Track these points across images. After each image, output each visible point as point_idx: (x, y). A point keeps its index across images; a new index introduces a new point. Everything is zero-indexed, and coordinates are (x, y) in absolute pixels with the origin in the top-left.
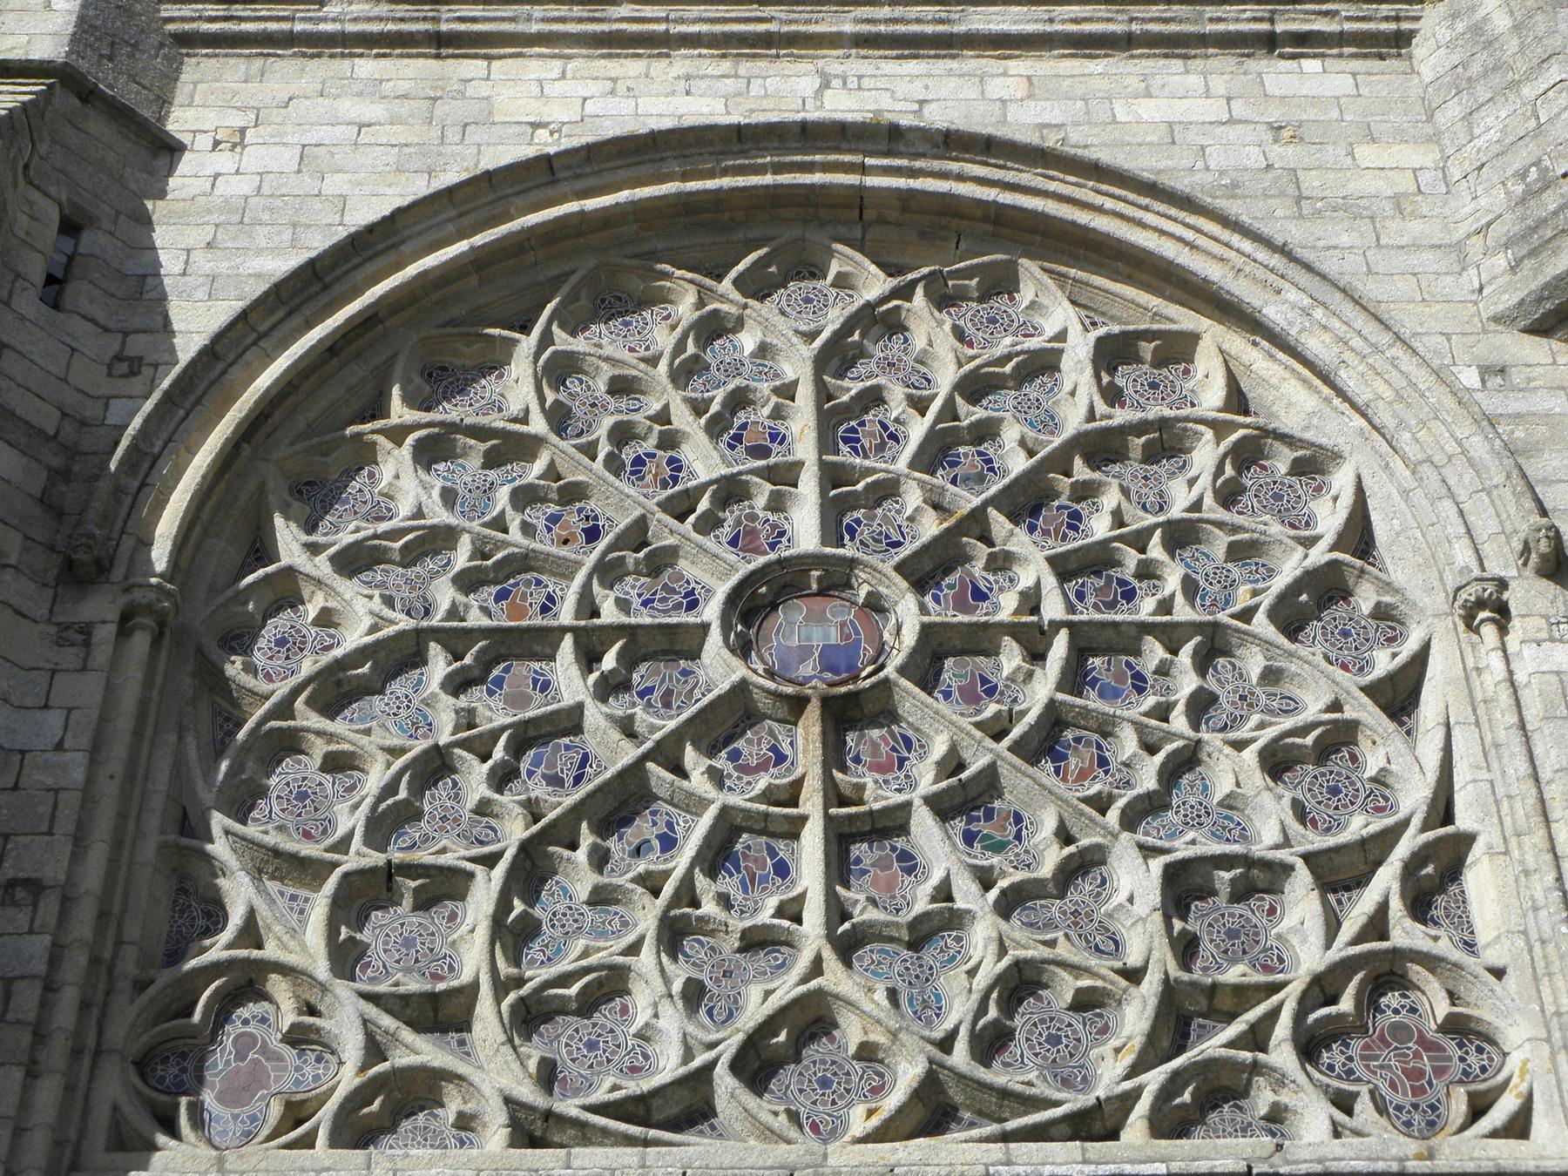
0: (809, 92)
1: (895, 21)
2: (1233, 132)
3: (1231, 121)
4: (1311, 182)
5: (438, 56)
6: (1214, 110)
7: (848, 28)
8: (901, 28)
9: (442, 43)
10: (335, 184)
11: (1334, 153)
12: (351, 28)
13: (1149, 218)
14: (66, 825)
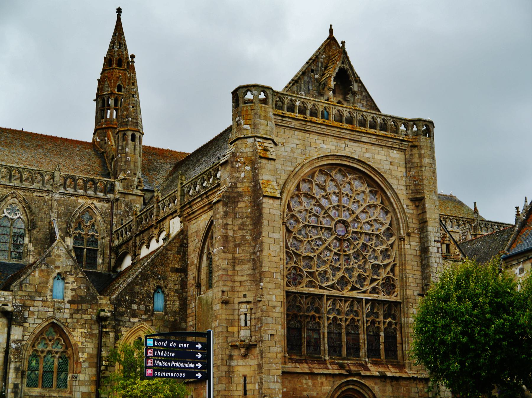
0: (344, 147)
1: (354, 138)
2: (386, 162)
3: (386, 160)
4: (394, 173)
5: (304, 133)
6: (384, 158)
7: (349, 138)
8: (355, 139)
9: (306, 131)
10: (295, 155)
11: (396, 168)
12: (296, 127)
13: (377, 176)
14: (282, 251)
